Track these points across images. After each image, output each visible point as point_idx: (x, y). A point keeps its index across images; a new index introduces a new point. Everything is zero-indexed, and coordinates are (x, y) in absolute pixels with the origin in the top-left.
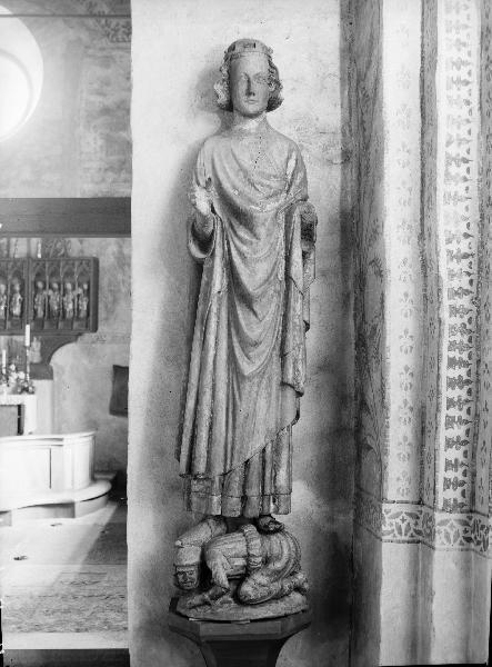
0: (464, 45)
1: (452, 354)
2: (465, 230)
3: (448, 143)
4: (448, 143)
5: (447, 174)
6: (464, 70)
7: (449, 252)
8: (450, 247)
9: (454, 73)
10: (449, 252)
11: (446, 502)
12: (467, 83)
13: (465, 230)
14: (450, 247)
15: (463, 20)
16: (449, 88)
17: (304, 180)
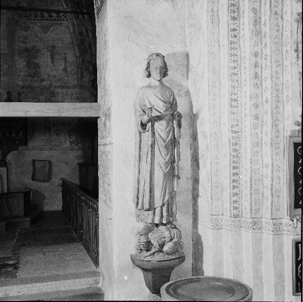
0: (237, 61)
1: (234, 165)
2: (236, 123)
3: (232, 94)
4: (232, 94)
5: (231, 105)
6: (236, 70)
7: (232, 131)
8: (232, 129)
9: (233, 71)
10: (232, 131)
11: (234, 214)
12: (237, 74)
13: (236, 123)
14: (232, 129)
15: (235, 53)
16: (231, 76)
17: (176, 103)
